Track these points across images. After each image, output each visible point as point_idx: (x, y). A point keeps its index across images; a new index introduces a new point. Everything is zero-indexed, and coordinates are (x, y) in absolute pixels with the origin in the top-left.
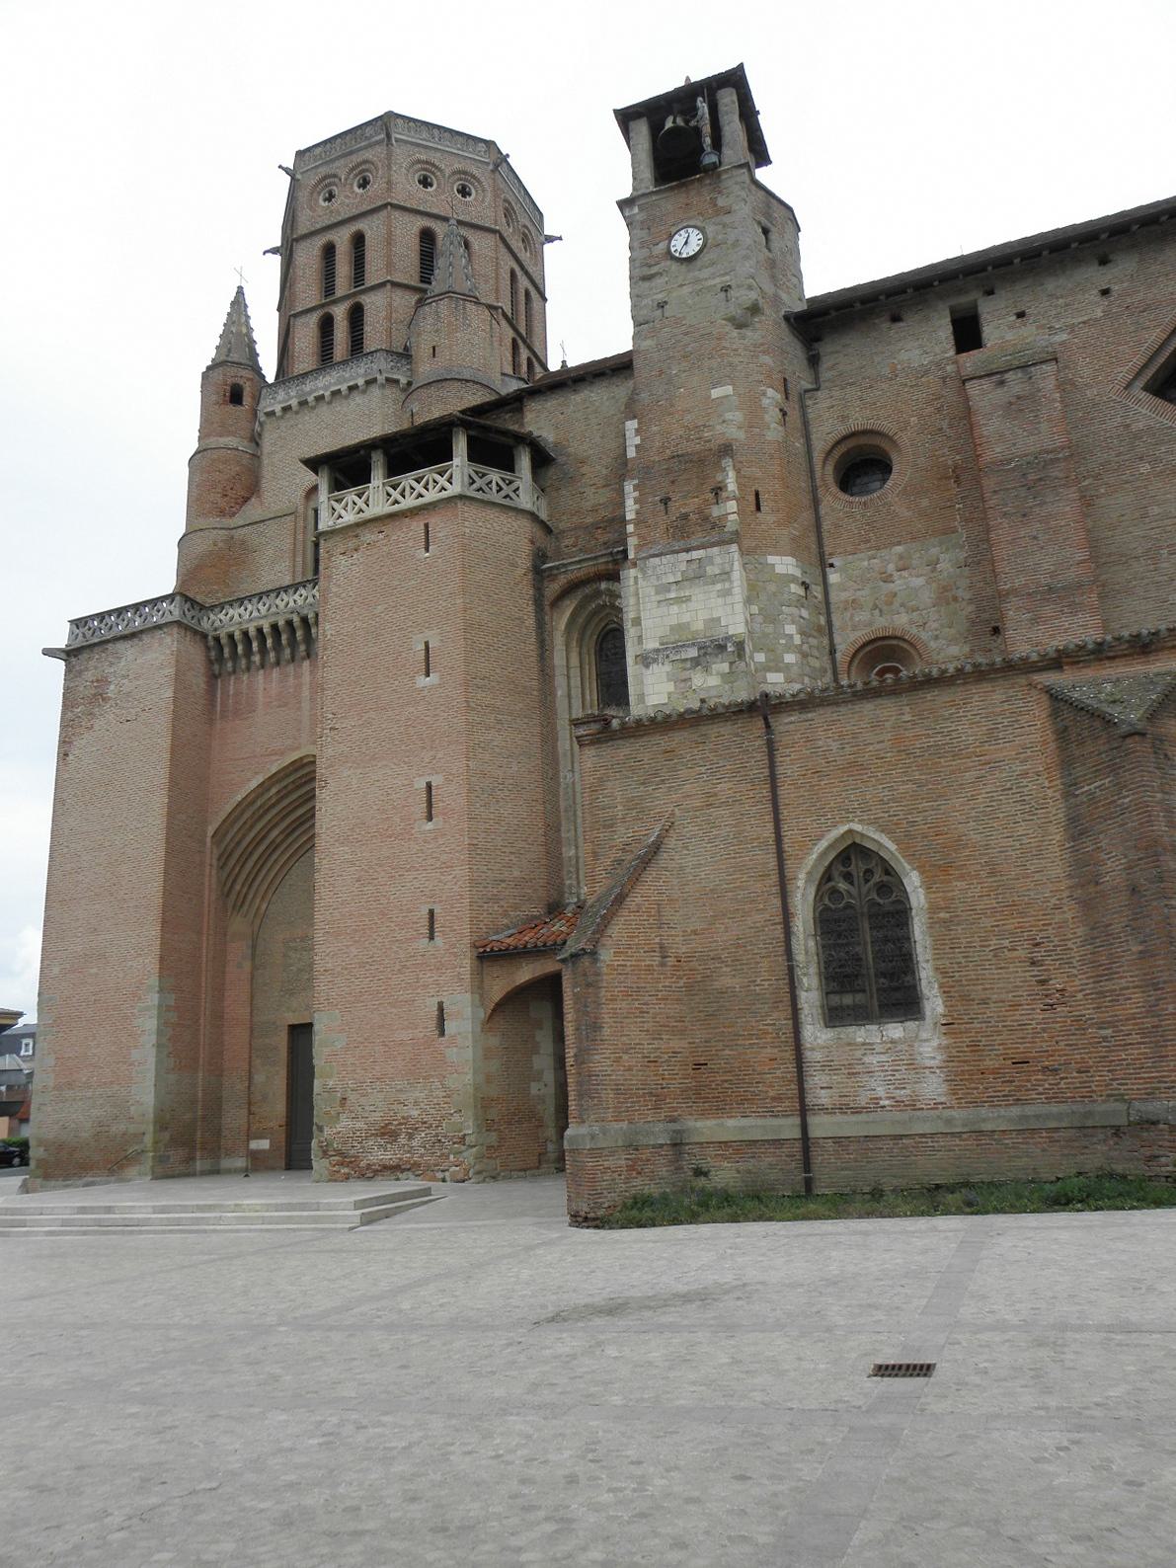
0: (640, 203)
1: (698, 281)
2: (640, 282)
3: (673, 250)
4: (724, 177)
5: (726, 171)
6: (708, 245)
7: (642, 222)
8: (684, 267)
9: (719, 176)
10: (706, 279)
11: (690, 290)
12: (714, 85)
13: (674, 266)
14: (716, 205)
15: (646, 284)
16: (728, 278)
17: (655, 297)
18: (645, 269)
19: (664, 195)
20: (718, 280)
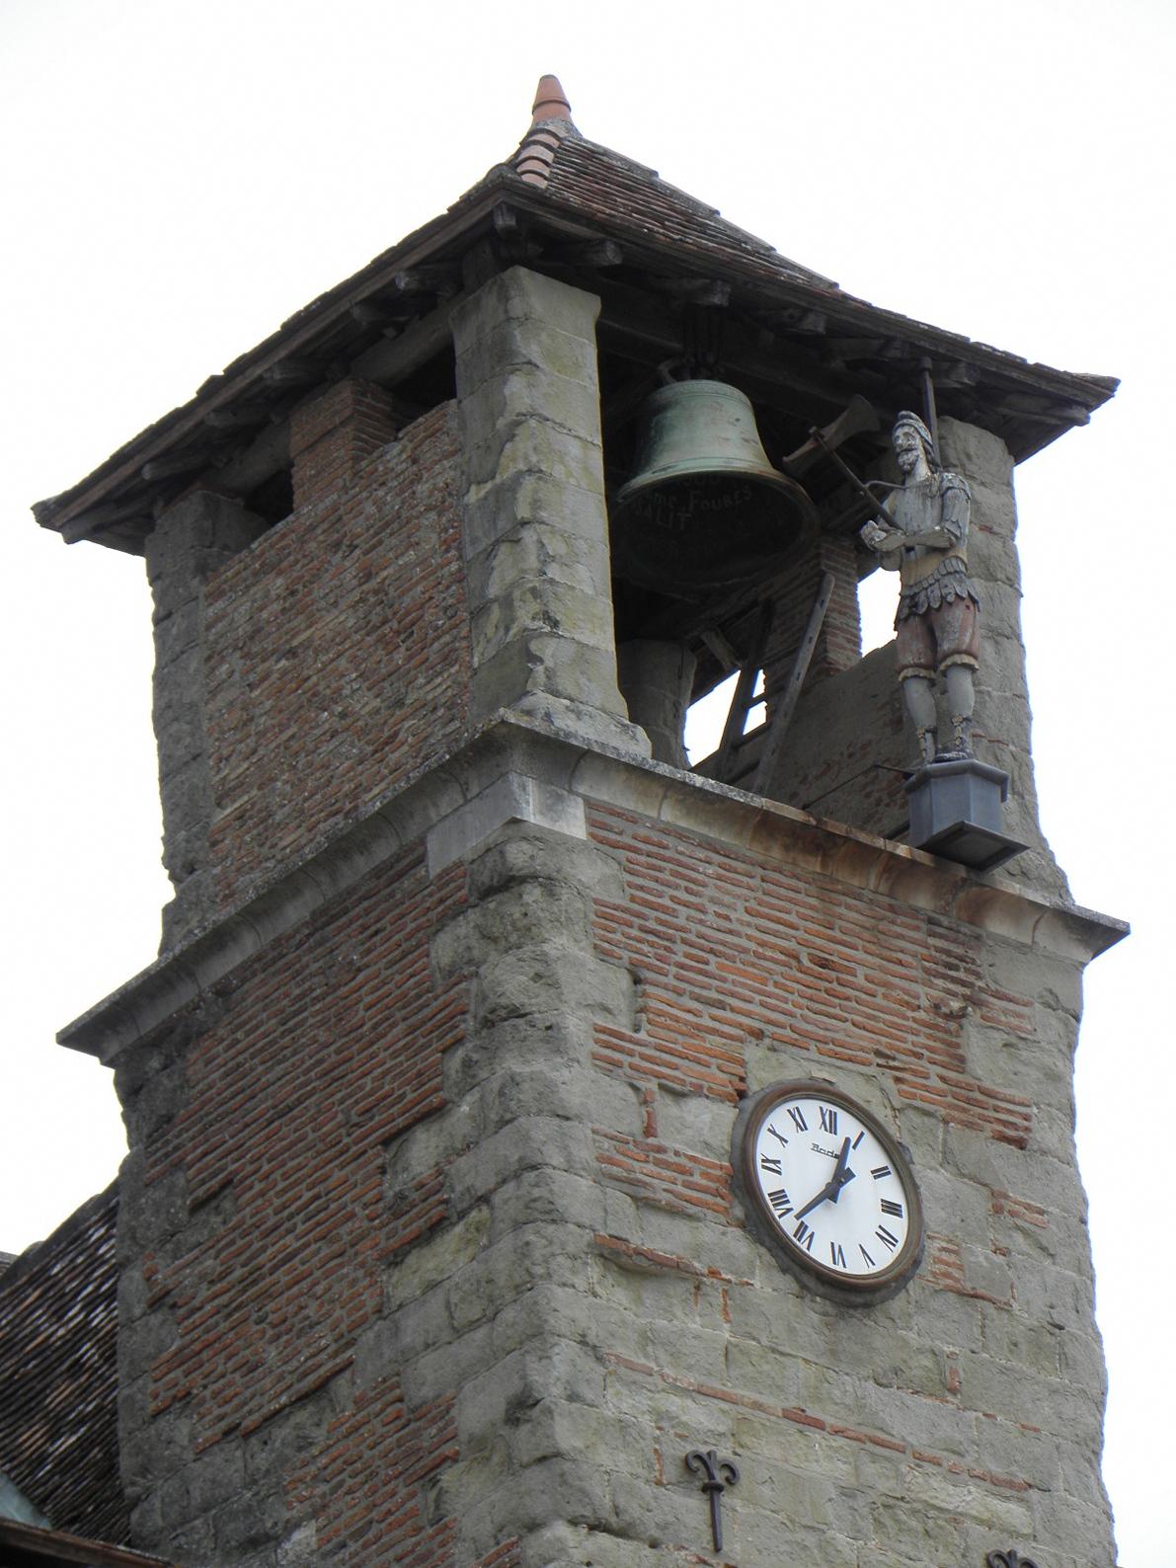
0: (604, 794)
1: (877, 1442)
2: (594, 1271)
3: (768, 1182)
4: (997, 926)
5: (1021, 908)
6: (927, 1267)
7: (607, 915)
8: (808, 1317)
9: (976, 911)
10: (919, 1458)
11: (842, 1470)
12: (963, 378)
13: (767, 1285)
14: (960, 1063)
15: (617, 1296)
16: (1012, 1512)
17: (674, 1404)
18: (619, 1200)
19: (726, 838)
20: (969, 1498)
